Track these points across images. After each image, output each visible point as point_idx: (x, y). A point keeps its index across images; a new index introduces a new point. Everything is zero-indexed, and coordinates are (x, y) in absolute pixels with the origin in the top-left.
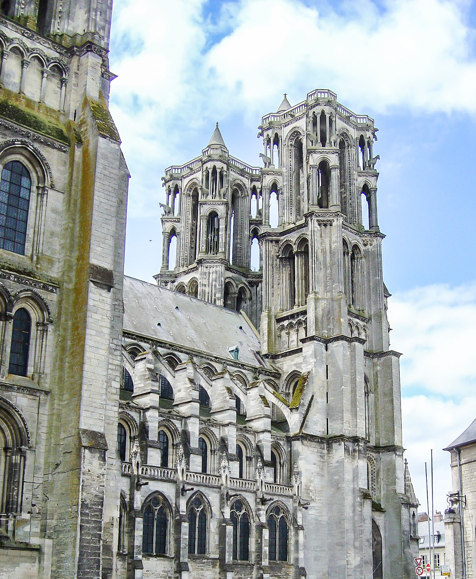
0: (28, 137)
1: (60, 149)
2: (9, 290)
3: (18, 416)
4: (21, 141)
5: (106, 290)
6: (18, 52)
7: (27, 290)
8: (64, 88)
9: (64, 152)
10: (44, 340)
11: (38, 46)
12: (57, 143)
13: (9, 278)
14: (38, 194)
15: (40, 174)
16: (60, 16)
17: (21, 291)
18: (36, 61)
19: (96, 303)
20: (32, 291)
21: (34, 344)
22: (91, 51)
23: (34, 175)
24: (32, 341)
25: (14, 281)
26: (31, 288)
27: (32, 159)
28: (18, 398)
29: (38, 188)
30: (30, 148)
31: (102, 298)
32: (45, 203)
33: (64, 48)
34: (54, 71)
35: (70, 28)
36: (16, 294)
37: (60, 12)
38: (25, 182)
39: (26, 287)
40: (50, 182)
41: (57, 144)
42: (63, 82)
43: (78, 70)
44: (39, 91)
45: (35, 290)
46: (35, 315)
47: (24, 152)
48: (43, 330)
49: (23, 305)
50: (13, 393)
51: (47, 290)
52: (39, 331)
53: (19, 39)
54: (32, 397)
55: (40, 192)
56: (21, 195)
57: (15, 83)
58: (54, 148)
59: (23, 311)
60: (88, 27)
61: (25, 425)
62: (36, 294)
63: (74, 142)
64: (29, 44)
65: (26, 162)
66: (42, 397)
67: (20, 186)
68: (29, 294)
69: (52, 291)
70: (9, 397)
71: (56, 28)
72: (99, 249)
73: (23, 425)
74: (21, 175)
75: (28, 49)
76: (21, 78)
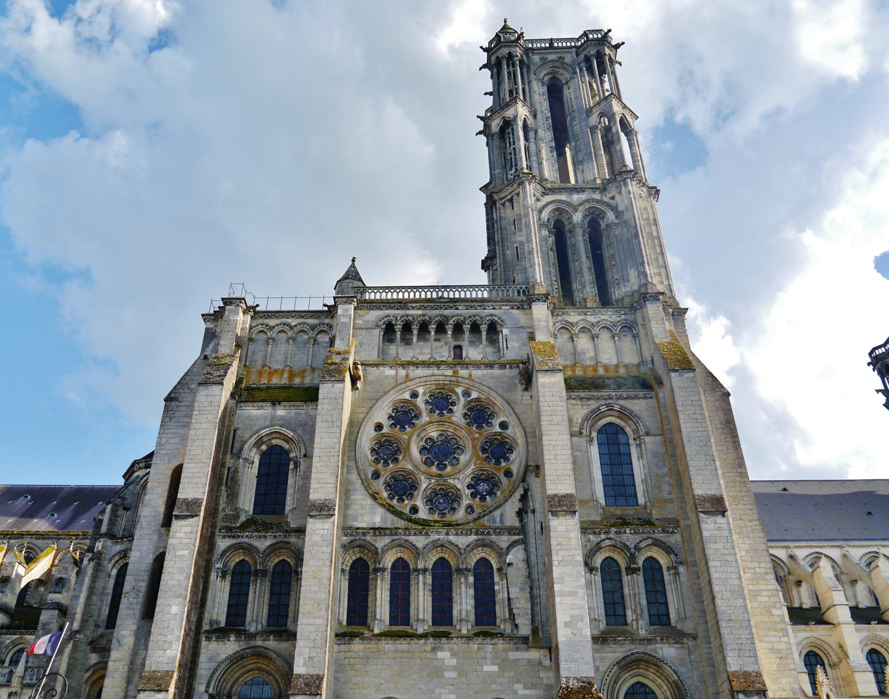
0: (611, 398)
1: (645, 398)
2: (628, 543)
3: (668, 668)
4: (605, 405)
5: (720, 516)
6: (586, 330)
7: (647, 539)
8: (637, 341)
9: (651, 398)
10: (678, 583)
11: (603, 317)
12: (641, 393)
13: (625, 532)
14: (637, 445)
15: (634, 427)
16: (617, 282)
17: (641, 541)
18: (605, 330)
19: (711, 532)
20: (651, 538)
21: (670, 589)
22: (648, 300)
23: (628, 430)
24: (668, 587)
25: (631, 533)
26: (650, 535)
27: (622, 416)
28: (664, 650)
29: (635, 439)
30: (617, 408)
31: (717, 525)
32: (644, 451)
33: (627, 308)
34: (625, 331)
35: (628, 289)
36: (635, 546)
37: (616, 279)
38: (621, 438)
39: (645, 536)
40: (644, 430)
41: (641, 394)
42: (635, 337)
43: (644, 321)
44: (615, 354)
45: (655, 536)
46: (663, 560)
47: (612, 413)
48: (675, 573)
49: (649, 554)
50: (658, 645)
51: (668, 532)
52: (672, 576)
53: (583, 320)
54: (678, 646)
55: (638, 442)
56: (622, 452)
57: (591, 357)
58: (639, 398)
59: (650, 559)
60: (640, 281)
61: (679, 677)
62: (656, 539)
63: (655, 387)
64: (592, 319)
65: (617, 421)
66: (691, 643)
67: (618, 444)
68: (650, 541)
69: (673, 532)
70: (655, 650)
71: (617, 295)
72: (700, 478)
73: (676, 678)
74: (617, 434)
75: (593, 324)
76: (595, 350)
